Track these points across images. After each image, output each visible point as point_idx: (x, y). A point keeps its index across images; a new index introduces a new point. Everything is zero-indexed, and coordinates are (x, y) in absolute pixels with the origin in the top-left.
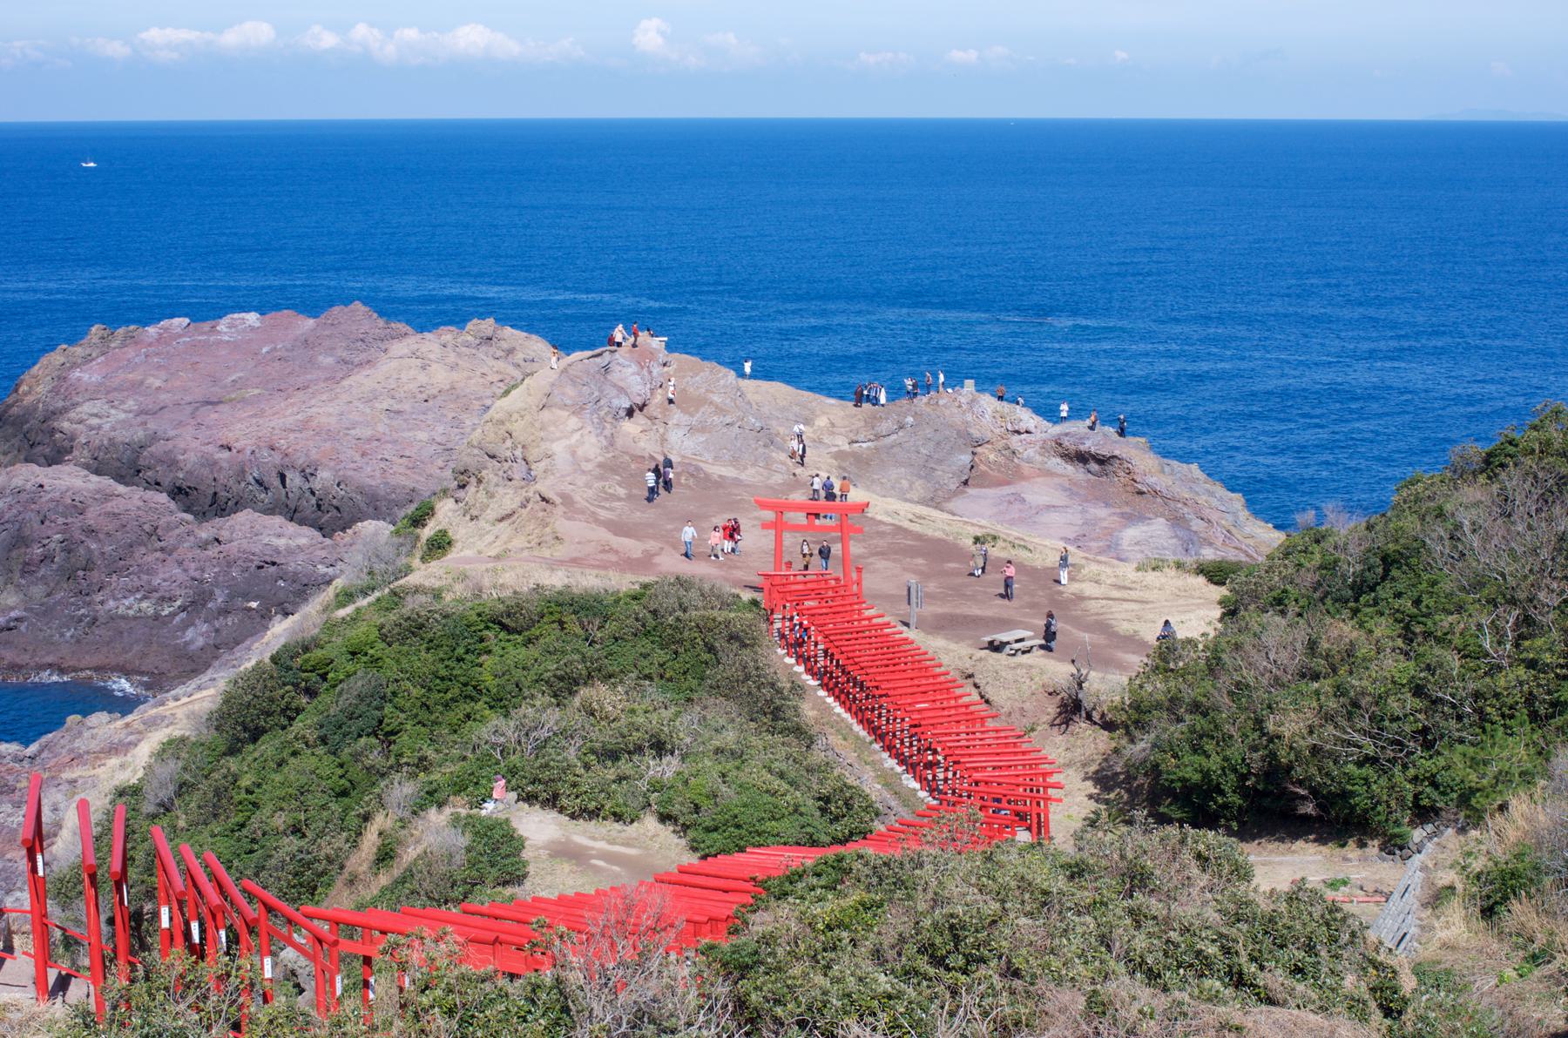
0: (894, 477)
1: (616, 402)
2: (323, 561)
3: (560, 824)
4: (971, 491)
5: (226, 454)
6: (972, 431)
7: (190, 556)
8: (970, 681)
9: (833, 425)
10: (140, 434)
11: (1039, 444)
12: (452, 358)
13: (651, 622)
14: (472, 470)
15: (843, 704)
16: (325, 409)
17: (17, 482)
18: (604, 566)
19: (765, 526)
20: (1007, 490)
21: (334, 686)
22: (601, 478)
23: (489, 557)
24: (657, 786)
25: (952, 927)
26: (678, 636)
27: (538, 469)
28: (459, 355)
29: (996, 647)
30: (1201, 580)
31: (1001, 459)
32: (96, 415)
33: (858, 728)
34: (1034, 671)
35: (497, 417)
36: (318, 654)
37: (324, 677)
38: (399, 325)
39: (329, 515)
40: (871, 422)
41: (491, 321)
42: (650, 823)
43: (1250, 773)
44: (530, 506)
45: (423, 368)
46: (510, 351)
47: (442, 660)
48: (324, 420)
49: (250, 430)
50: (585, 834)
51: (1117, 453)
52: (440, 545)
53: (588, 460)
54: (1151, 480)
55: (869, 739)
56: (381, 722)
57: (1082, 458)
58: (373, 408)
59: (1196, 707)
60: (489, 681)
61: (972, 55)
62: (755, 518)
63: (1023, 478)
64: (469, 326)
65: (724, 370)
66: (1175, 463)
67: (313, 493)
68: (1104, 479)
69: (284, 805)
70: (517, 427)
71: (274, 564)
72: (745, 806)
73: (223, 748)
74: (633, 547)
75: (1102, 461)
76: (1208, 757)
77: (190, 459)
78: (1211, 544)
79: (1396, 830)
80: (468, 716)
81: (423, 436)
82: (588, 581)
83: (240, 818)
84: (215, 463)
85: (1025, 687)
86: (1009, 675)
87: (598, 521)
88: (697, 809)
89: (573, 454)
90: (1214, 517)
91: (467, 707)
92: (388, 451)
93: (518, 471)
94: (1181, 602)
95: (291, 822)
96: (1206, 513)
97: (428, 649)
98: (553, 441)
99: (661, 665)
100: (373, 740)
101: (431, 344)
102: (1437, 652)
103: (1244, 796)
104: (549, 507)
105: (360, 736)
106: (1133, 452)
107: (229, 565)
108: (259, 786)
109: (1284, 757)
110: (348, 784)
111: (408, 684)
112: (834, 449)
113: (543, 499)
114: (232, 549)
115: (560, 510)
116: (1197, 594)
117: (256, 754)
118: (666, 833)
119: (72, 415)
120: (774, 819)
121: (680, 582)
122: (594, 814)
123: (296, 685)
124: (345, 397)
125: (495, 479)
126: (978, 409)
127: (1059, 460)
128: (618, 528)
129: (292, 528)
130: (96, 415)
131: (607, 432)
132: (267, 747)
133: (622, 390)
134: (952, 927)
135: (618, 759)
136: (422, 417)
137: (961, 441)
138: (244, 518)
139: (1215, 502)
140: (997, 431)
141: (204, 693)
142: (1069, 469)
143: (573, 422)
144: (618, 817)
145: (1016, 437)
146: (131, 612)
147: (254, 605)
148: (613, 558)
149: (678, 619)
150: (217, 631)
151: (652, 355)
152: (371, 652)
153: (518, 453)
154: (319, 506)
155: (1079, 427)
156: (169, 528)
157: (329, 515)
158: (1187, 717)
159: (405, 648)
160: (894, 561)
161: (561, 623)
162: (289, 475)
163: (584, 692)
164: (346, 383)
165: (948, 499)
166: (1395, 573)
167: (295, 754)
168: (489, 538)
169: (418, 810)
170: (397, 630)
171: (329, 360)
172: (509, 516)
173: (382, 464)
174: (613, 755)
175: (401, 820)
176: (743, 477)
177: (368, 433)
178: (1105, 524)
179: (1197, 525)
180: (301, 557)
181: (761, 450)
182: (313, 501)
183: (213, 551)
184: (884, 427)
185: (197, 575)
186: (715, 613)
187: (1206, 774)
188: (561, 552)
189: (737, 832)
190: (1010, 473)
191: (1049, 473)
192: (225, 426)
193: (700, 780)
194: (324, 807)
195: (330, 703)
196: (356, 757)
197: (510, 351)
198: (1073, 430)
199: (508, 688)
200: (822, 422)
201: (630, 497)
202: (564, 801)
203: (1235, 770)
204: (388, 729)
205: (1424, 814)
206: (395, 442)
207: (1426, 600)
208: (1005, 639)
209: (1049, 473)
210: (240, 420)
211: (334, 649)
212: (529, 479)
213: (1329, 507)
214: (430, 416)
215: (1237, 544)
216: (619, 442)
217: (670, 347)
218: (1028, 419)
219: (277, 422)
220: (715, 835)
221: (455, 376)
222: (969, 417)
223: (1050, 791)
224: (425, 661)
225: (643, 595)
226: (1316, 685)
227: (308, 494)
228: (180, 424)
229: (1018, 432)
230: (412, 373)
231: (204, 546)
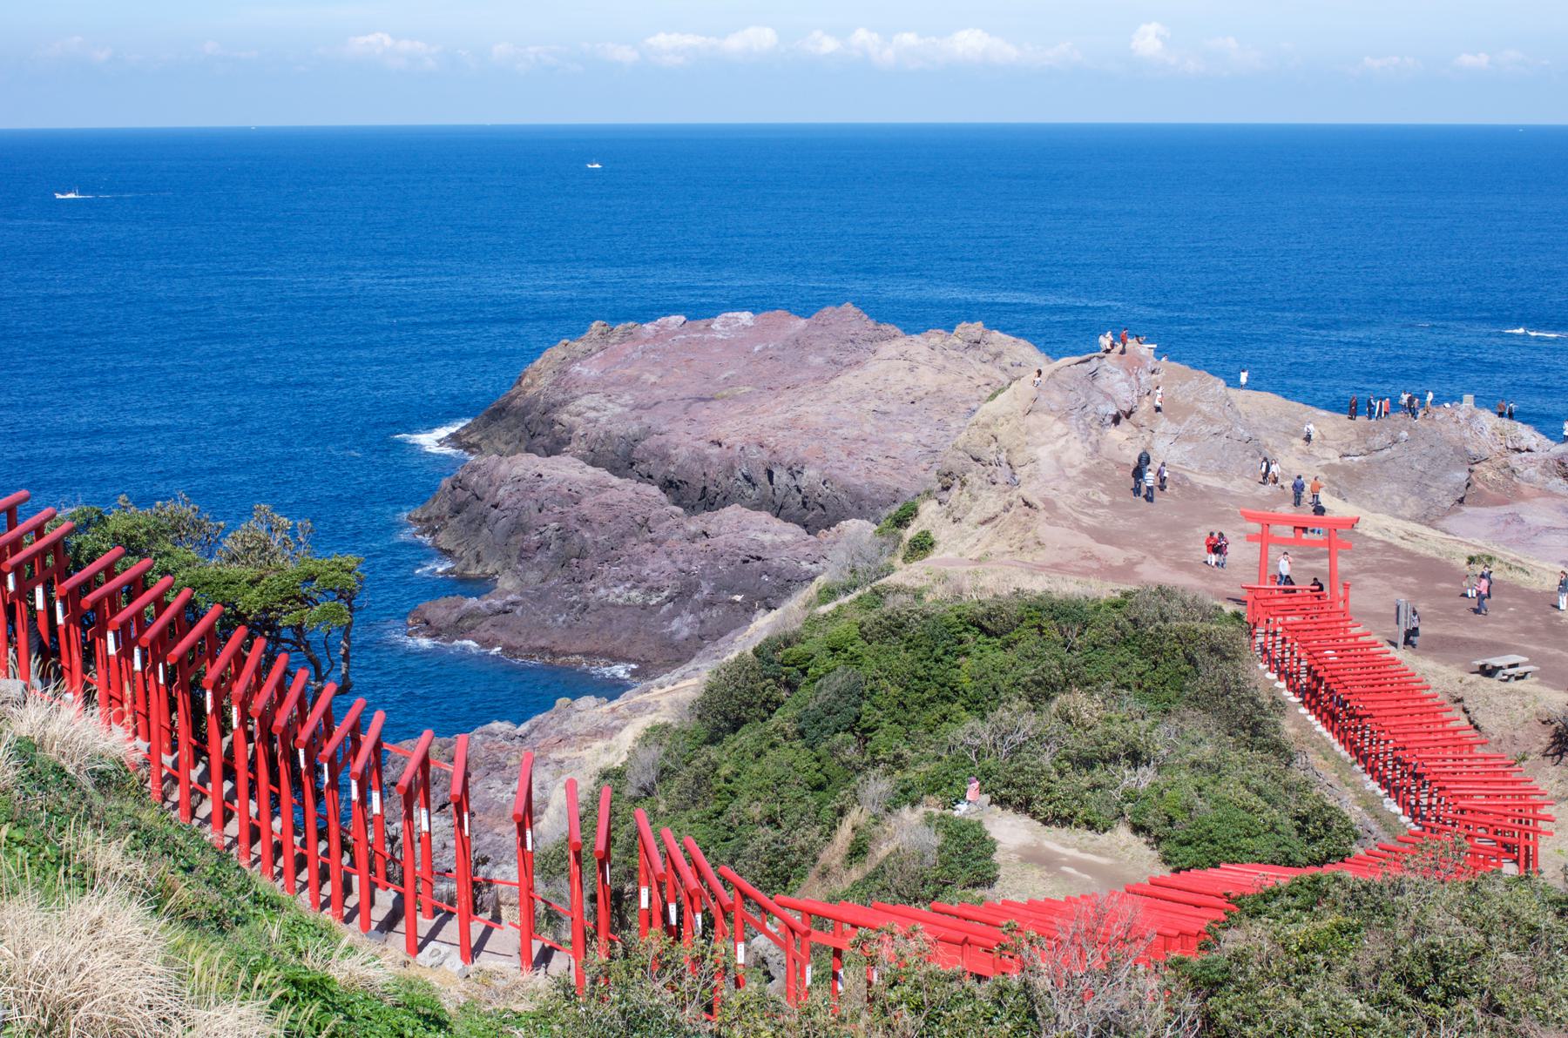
0: (1385, 492)
1: (1102, 409)
3: (1032, 829)
4: (1466, 509)
5: (716, 450)
6: (1469, 447)
7: (678, 548)
8: (1459, 705)
10: (635, 428)
12: (940, 361)
13: (1131, 631)
14: (956, 472)
15: (1324, 722)
16: (814, 409)
17: (518, 471)
18: (1086, 573)
19: (1250, 538)
20: (1504, 510)
21: (814, 681)
22: (1086, 484)
23: (969, 560)
24: (1131, 797)
25: (1432, 957)
26: (1158, 646)
27: (1022, 473)
29: (1487, 672)
31: (1500, 478)
32: (594, 409)
33: (1339, 748)
34: (1527, 699)
35: (983, 420)
36: (799, 649)
37: (804, 672)
39: (815, 513)
40: (1363, 435)
41: (980, 324)
42: (1123, 833)
44: (1013, 510)
45: (911, 370)
46: (998, 355)
48: (812, 418)
49: (740, 427)
50: (1057, 841)
52: (922, 546)
53: (1072, 466)
55: (1350, 759)
56: (858, 718)
58: (860, 408)
60: (966, 683)
61: (1483, 60)
64: (958, 329)
67: (799, 491)
69: (761, 795)
70: (1002, 431)
71: (759, 558)
73: (704, 737)
74: (1115, 555)
77: (682, 454)
80: (944, 717)
81: (908, 437)
82: (1069, 587)
83: (718, 806)
84: (706, 458)
85: (1517, 715)
86: (1501, 701)
87: (1080, 528)
88: (1171, 821)
89: (1058, 459)
91: (944, 708)
92: (874, 451)
93: (1002, 475)
95: (767, 812)
97: (907, 649)
98: (1038, 446)
99: (1140, 675)
100: (850, 736)
101: (920, 346)
104: (1031, 512)
105: (837, 731)
107: (716, 558)
108: (737, 775)
112: (1325, 462)
113: (1027, 504)
114: (719, 542)
115: (1043, 515)
117: (736, 744)
118: (1138, 844)
119: (571, 407)
120: (1249, 835)
121: (1163, 592)
122: (1066, 821)
123: (777, 679)
124: (833, 397)
126: (1475, 425)
127: (1561, 480)
128: (1100, 535)
129: (777, 524)
130: (594, 409)
131: (1093, 439)
132: (746, 738)
133: (1109, 397)
135: (1093, 767)
136: (908, 418)
137: (1457, 458)
138: (732, 512)
140: (1497, 448)
141: (688, 682)
143: (1059, 428)
144: (1091, 825)
145: (1517, 455)
146: (620, 601)
147: (738, 598)
148: (1095, 565)
149: (1158, 629)
150: (702, 622)
151: (1140, 361)
153: (1003, 457)
154: (804, 504)
156: (659, 520)
157: (815, 513)
159: (885, 646)
160: (1383, 578)
161: (1040, 628)
162: (776, 472)
163: (1061, 698)
164: (834, 383)
165: (1442, 517)
167: (773, 746)
168: (972, 540)
169: (892, 807)
170: (877, 628)
171: (817, 361)
173: (868, 464)
174: (1088, 763)
175: (875, 816)
176: (1229, 488)
177: (854, 433)
180: (785, 553)
181: (1249, 461)
182: (799, 498)
183: (700, 544)
184: (1377, 441)
185: (685, 566)
186: (1197, 624)
188: (1042, 557)
189: (1211, 847)
190: (1509, 492)
191: (1550, 494)
192: (716, 422)
195: (810, 698)
196: (833, 751)
197: (998, 355)
199: (986, 691)
201: (1113, 504)
202: (1037, 807)
208: (1498, 664)
209: (1550, 494)
210: (731, 417)
211: (815, 644)
212: (1013, 483)
214: (916, 418)
216: (1105, 449)
217: (1159, 353)
218: (1528, 435)
219: (767, 420)
220: (1188, 849)
221: (942, 378)
222: (1467, 434)
223: (1540, 823)
224: (902, 660)
225: (1124, 603)
227: (794, 491)
228: (673, 419)
229: (1519, 450)
230: (900, 374)
231: (692, 539)
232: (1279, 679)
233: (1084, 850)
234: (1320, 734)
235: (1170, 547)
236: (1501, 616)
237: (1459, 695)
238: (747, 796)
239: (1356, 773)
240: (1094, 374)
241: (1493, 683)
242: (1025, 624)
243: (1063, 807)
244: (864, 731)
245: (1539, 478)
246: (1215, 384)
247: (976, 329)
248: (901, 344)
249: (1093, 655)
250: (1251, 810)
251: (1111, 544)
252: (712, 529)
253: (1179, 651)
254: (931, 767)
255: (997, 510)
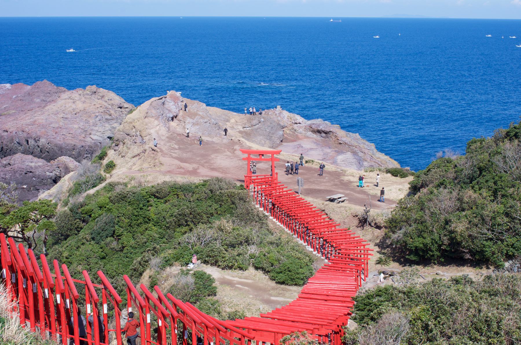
0: (259, 139)
1: (168, 115)
2: (48, 171)
3: (219, 272)
4: (284, 144)
5: (6, 134)
8: (323, 213)
9: (237, 122)
11: (304, 127)
12: (83, 99)
13: (211, 195)
16: (41, 117)
21: (94, 219)
22: (169, 142)
23: (129, 171)
24: (252, 256)
25: (486, 321)
26: (221, 199)
27: (146, 139)
28: (85, 98)
29: (332, 200)
30: (389, 175)
31: (291, 133)
33: (287, 230)
35: (129, 121)
37: (90, 216)
38: (62, 88)
39: (48, 154)
40: (249, 120)
41: (95, 86)
42: (251, 270)
43: (443, 244)
44: (147, 153)
45: (74, 103)
46: (103, 97)
47: (135, 209)
48: (40, 121)
51: (331, 130)
52: (111, 166)
53: (163, 136)
54: (344, 139)
55: (291, 234)
56: (114, 231)
57: (319, 132)
59: (416, 221)
60: (153, 216)
62: (226, 155)
63: (299, 139)
64: (88, 88)
65: (202, 103)
66: (350, 133)
67: (39, 147)
68: (327, 139)
70: (137, 124)
71: (31, 172)
72: (291, 264)
74: (189, 167)
75: (326, 133)
76: (424, 238)
78: (366, 161)
79: (500, 263)
80: (146, 229)
81: (76, 126)
82: (181, 180)
84: (2, 137)
86: (338, 210)
87: (172, 157)
89: (158, 133)
90: (366, 151)
91: (146, 226)
92: (64, 132)
93: (139, 139)
94: (384, 182)
96: (363, 150)
98: (150, 129)
99: (216, 209)
100: (112, 238)
101: (76, 94)
102: (511, 202)
103: (440, 251)
104: (155, 153)
106: (337, 130)
107: (15, 173)
108: (71, 256)
109: (459, 239)
110: (105, 255)
111: (123, 218)
113: (153, 150)
115: (160, 154)
116: (389, 180)
118: (260, 273)
120: (301, 268)
121: (219, 180)
122: (231, 268)
123: (80, 219)
124: (47, 113)
125: (130, 143)
126: (282, 115)
127: (311, 133)
129: (36, 159)
131: (167, 126)
132: (72, 241)
133: (170, 111)
134: (486, 321)
135: (235, 247)
136: (75, 120)
137: (279, 127)
138: (18, 156)
139: (366, 147)
140: (289, 123)
142: (315, 136)
143: (156, 122)
144: (241, 269)
145: (296, 125)
147: (25, 187)
148: (183, 171)
149: (220, 193)
152: (107, 206)
153: (138, 133)
154: (41, 151)
155: (319, 121)
157: (48, 154)
158: (413, 224)
159: (120, 205)
160: (280, 169)
161: (178, 195)
162: (30, 141)
164: (47, 108)
166: (484, 173)
167: (83, 244)
168: (130, 164)
171: (38, 100)
172: (136, 156)
174: (233, 246)
177: (57, 125)
178: (331, 154)
179: (361, 154)
180: (40, 170)
181: (217, 131)
182: (39, 149)
183: (8, 168)
184: (255, 122)
185: (4, 176)
186: (234, 190)
187: (425, 245)
188: (164, 169)
189: (290, 273)
190: (295, 138)
191: (308, 137)
192: (4, 123)
193: (271, 254)
194: (97, 263)
196: (107, 245)
197: (103, 97)
198: (315, 122)
200: (233, 121)
202: (220, 264)
203: (436, 243)
204: (118, 234)
205: (509, 257)
206: (66, 128)
207: (499, 183)
208: (335, 198)
209: (308, 137)
210: (9, 121)
211: (92, 205)
212: (143, 143)
213: (446, 150)
214: (78, 119)
215: (375, 161)
216: (171, 129)
218: (299, 119)
220: (281, 274)
221: (85, 105)
222: (279, 118)
223: (369, 252)
225: (206, 184)
226: (464, 213)
227: (37, 147)
229: (296, 123)
230: (70, 104)
232: (261, 207)
233: (240, 278)
234: (279, 225)
235: (206, 162)
236: (325, 180)
237: (323, 209)
238: (76, 263)
239: (295, 238)
240: (163, 103)
241: (334, 204)
242: (172, 194)
243: (229, 263)
244: (117, 236)
245: (304, 132)
246: (202, 105)
247: (94, 88)
248: (67, 94)
249: (199, 203)
250: (299, 259)
251: (186, 163)
252: (12, 162)
253: (229, 200)
254: (175, 252)
255: (138, 152)
